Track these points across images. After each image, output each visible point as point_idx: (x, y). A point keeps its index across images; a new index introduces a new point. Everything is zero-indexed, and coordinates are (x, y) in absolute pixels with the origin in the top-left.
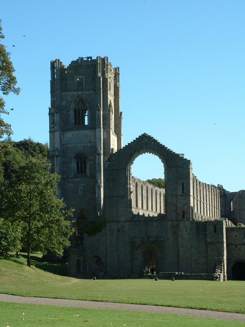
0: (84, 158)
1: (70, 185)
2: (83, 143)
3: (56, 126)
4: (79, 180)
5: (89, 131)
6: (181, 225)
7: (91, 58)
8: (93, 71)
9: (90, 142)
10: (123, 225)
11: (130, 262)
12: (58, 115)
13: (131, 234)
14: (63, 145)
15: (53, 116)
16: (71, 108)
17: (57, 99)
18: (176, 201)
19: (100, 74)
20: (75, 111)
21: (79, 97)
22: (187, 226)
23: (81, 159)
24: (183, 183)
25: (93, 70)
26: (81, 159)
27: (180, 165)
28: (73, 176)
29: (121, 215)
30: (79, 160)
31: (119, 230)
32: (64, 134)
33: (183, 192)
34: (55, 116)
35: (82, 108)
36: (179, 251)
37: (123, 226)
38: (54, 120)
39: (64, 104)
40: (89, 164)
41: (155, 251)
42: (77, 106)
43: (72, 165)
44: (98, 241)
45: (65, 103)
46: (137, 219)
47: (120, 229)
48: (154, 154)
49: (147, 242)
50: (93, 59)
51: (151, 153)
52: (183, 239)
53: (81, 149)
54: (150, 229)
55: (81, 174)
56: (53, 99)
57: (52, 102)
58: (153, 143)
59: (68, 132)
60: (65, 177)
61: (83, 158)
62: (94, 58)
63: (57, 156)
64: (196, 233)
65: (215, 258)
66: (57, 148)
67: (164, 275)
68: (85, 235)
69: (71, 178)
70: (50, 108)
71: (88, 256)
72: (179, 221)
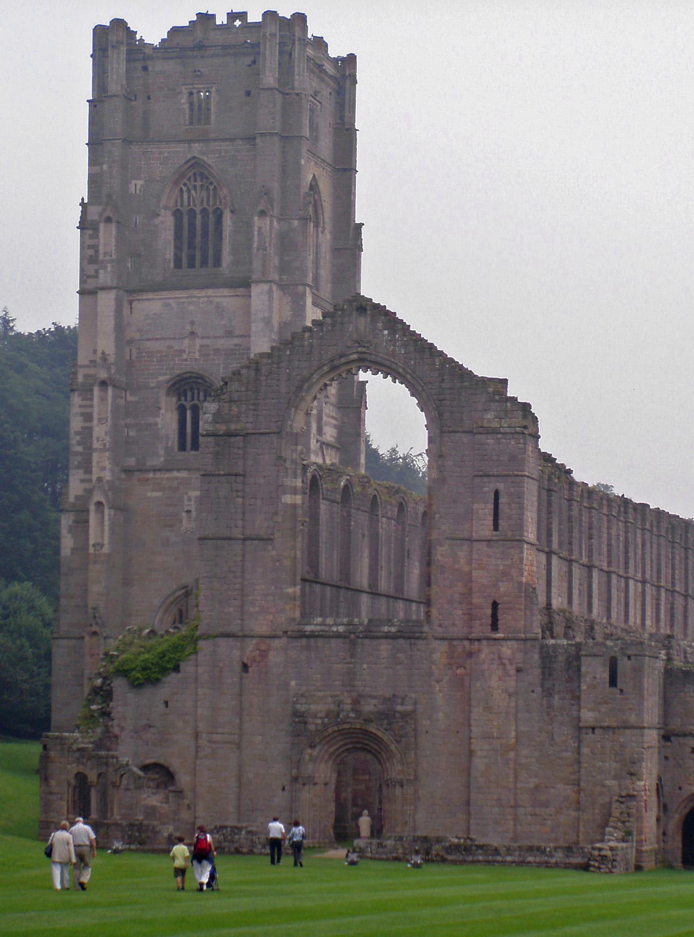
1: (149, 494)
2: (203, 338)
3: (101, 271)
4: (183, 474)
5: (226, 292)
6: (483, 656)
7: (243, 15)
8: (250, 66)
9: (229, 334)
10: (263, 648)
11: (283, 789)
12: (113, 227)
13: (293, 683)
14: (130, 342)
15: (95, 235)
16: (163, 203)
17: (110, 167)
18: (470, 562)
19: (270, 79)
20: (177, 214)
21: (193, 161)
22: (504, 661)
23: (193, 399)
24: (497, 493)
26: (193, 399)
27: (489, 421)
28: (162, 459)
29: (257, 609)
30: (186, 400)
31: (245, 667)
32: (134, 300)
33: (496, 527)
34: (101, 234)
35: (202, 204)
36: (471, 754)
37: (264, 654)
38: (95, 247)
39: (138, 187)
41: (383, 754)
42: (185, 196)
43: (159, 420)
44: (167, 706)
45: (140, 183)
46: (318, 628)
47: (249, 664)
48: (389, 378)
49: (352, 715)
50: (249, 21)
51: (380, 375)
52: (488, 708)
53: (196, 360)
54: (365, 666)
55: (193, 453)
56: (96, 169)
57: (94, 181)
58: (386, 332)
59: (151, 296)
60: (131, 462)
61: (202, 394)
62: (254, 17)
63: (103, 384)
64: (542, 685)
65: (607, 783)
66: (103, 353)
67: (403, 846)
68: (119, 685)
69: (155, 470)
70: (86, 201)
71: (118, 761)
72: (479, 640)
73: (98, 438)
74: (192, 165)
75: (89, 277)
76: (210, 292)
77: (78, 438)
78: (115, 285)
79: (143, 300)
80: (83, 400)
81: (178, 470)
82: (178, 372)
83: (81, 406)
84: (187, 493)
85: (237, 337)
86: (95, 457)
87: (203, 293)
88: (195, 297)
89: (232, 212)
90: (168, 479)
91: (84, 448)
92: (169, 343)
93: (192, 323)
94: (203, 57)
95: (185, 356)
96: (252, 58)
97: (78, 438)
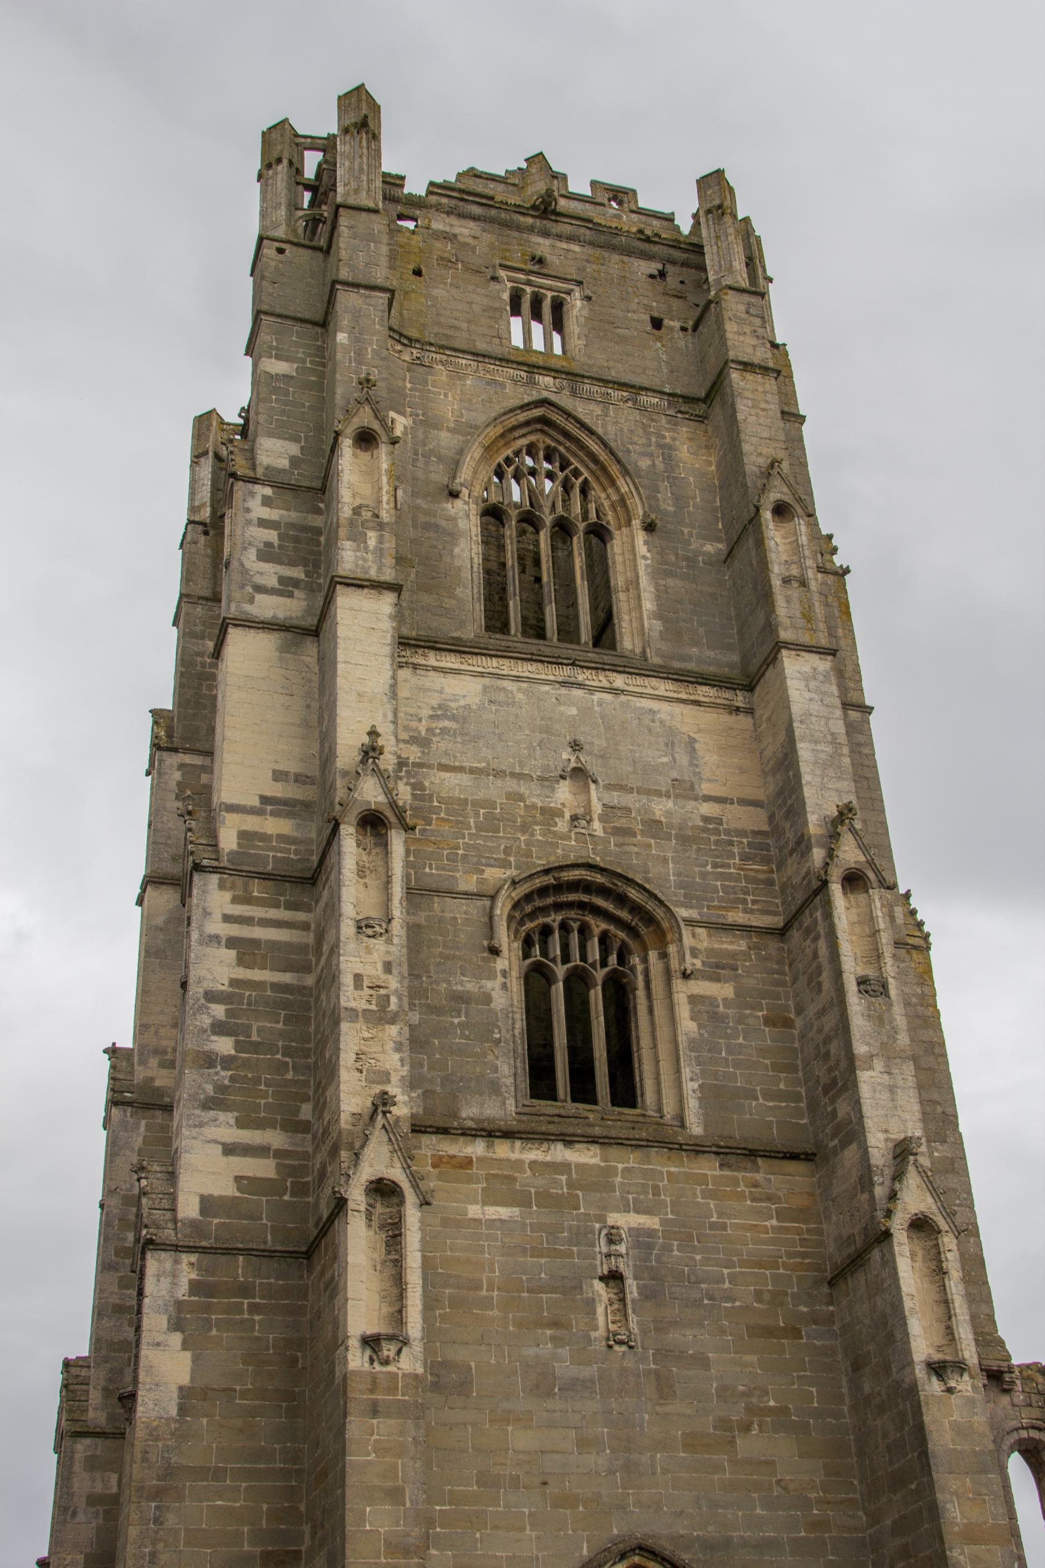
0: (604, 939)
1: (474, 1211)
2: (609, 787)
5: (663, 687)
7: (620, 195)
8: (652, 276)
9: (684, 789)
16: (465, 474)
21: (537, 412)
23: (566, 958)
25: (656, 273)
40: (693, 999)
43: (493, 986)
59: (450, 661)
66: (373, 733)
69: (491, 1133)
73: (358, 978)
74: (527, 423)
75: (259, 589)
76: (619, 681)
77: (219, 1011)
78: (388, 575)
79: (427, 668)
80: (235, 900)
81: (568, 1141)
82: (541, 863)
83: (227, 918)
84: (602, 1219)
85: (707, 798)
86: (351, 1038)
87: (602, 679)
88: (580, 686)
89: (650, 527)
90: (533, 1164)
91: (239, 1046)
92: (511, 785)
93: (576, 746)
94: (546, 234)
95: (562, 825)
96: (660, 267)
97: (219, 1011)
